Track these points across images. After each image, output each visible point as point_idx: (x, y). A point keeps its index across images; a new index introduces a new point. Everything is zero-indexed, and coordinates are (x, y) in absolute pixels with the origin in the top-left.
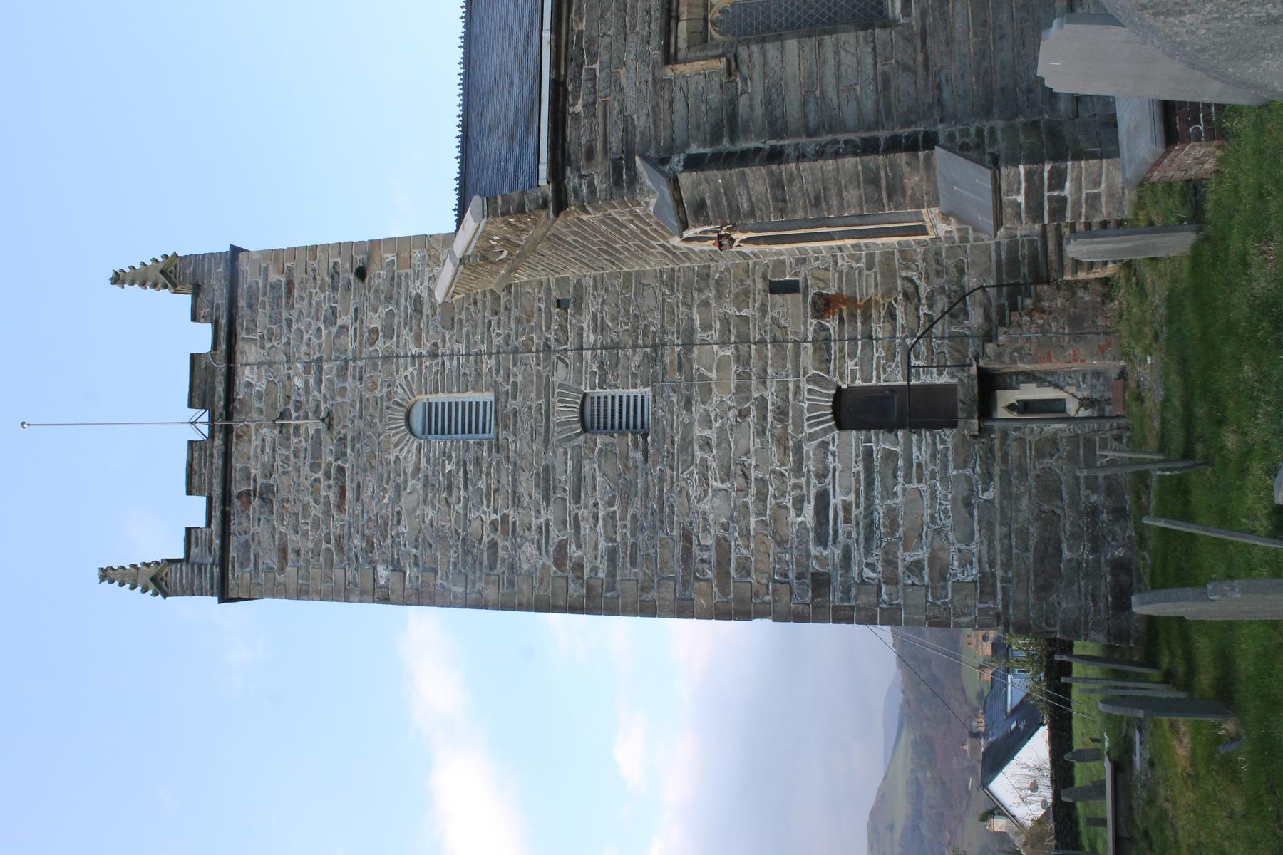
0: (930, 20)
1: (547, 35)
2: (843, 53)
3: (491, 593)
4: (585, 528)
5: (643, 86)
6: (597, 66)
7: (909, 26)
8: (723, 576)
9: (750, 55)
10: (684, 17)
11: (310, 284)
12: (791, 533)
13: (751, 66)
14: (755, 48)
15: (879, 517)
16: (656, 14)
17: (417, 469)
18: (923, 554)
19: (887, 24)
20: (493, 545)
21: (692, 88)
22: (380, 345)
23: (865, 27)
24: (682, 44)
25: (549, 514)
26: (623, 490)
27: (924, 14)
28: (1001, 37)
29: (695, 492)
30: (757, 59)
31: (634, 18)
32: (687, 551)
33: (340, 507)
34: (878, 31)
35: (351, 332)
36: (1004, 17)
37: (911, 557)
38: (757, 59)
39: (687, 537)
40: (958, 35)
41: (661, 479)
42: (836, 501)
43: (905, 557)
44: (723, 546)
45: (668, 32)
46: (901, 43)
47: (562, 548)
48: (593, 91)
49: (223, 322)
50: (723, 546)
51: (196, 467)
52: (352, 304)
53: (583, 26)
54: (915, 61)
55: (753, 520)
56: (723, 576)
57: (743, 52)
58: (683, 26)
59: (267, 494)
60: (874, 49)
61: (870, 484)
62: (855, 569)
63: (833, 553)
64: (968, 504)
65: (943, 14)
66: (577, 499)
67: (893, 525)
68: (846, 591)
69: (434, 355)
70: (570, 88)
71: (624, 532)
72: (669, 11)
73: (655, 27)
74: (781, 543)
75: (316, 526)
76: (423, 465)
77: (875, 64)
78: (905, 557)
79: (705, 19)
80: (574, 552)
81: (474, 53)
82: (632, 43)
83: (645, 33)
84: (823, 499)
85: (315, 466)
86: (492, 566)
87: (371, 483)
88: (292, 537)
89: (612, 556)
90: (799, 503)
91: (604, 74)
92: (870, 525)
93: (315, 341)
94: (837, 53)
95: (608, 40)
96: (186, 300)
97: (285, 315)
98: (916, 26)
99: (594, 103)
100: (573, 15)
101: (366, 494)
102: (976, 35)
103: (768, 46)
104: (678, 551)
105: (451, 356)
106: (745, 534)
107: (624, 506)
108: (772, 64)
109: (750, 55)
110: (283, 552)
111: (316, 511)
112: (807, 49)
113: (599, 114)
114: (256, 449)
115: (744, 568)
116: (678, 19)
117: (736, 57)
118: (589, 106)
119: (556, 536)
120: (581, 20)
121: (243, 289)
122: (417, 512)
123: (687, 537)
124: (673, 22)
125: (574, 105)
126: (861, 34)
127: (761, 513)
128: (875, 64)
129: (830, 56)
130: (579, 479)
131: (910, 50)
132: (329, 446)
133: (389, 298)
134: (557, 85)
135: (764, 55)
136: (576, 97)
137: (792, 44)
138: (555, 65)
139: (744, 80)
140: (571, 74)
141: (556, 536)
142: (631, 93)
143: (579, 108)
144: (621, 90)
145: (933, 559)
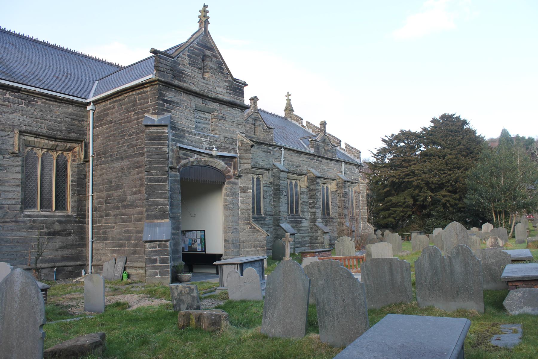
0: (21, 224)
1: (39, 90)
2: (14, 193)
5: (12, 121)
6: (23, 106)
7: (20, 217)
9: (18, 161)
10: (36, 140)
13: (14, 161)
14: (20, 163)
16: (39, 130)
19: (22, 209)
21: (9, 139)
23: (22, 202)
24: (26, 138)
27: (24, 222)
28: (12, 248)
30: (16, 164)
31: (39, 122)
34: (20, 206)
36: (19, 249)
38: (16, 164)
40: (14, 233)
45: (31, 133)
46: (14, 214)
48: (14, 103)
53: (39, 103)
54: (7, 218)
57: (19, 159)
58: (33, 139)
60: (14, 204)
65: (23, 228)
70: (17, 94)
72: (39, 135)
73: (34, 129)
77: (8, 205)
79: (34, 147)
81: (41, 46)
82: (30, 120)
83: (32, 125)
91: (20, 107)
94: (14, 191)
95: (33, 111)
98: (19, 219)
99: (9, 102)
100: (44, 100)
102: (13, 239)
103: (20, 168)
108: (13, 168)
109: (18, 161)
112: (17, 181)
113: (4, 103)
116: (35, 137)
117: (18, 156)
118: (8, 100)
120: (42, 103)
124: (35, 136)
125: (10, 94)
126: (20, 200)
128: (8, 205)
129: (13, 189)
131: (11, 217)
134: (19, 90)
135: (17, 166)
136: (12, 96)
137: (20, 176)
138: (27, 91)
139: (9, 158)
140: (22, 95)
142: (11, 116)
143: (8, 96)
144: (12, 113)
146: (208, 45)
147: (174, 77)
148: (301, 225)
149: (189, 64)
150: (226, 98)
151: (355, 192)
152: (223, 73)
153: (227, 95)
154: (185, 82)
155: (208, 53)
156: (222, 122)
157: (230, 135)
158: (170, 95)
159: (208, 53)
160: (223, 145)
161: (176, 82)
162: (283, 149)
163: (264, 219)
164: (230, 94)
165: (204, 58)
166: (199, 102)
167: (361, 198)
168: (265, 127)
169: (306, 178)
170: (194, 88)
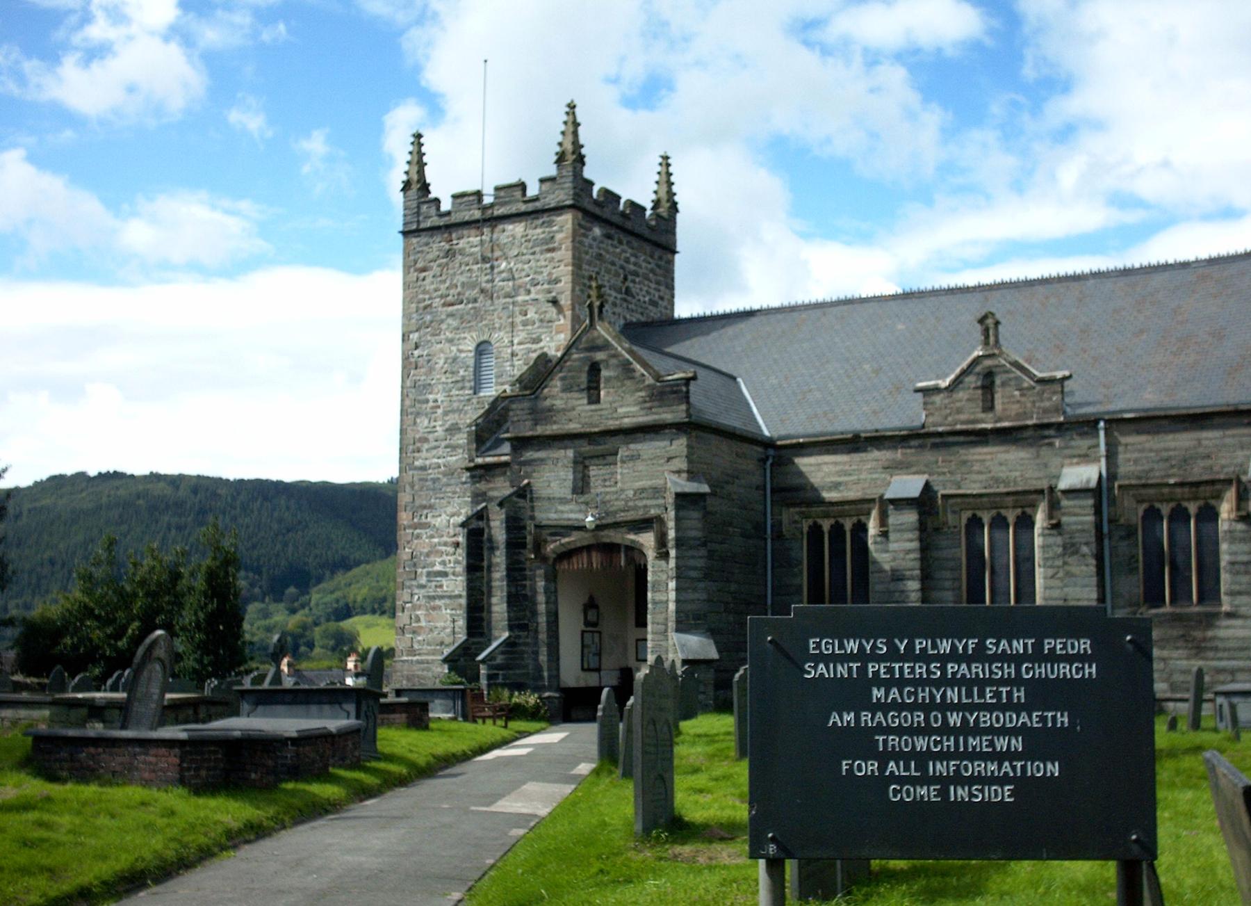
3: (407, 402)
4: (434, 452)
11: (552, 264)
12: (432, 559)
15: (438, 602)
17: (460, 351)
18: (423, 624)
20: (427, 401)
22: (519, 319)
26: (450, 473)
29: (450, 510)
32: (425, 507)
33: (444, 305)
35: (527, 298)
37: (422, 618)
39: (431, 507)
41: (454, 493)
42: (444, 582)
47: (426, 440)
49: (538, 205)
51: (466, 199)
52: (539, 297)
55: (436, 540)
59: (450, 254)
61: (450, 597)
62: (416, 591)
63: (423, 580)
64: (442, 643)
66: (446, 447)
67: (434, 608)
68: (409, 587)
69: (513, 355)
71: (433, 474)
74: (428, 555)
75: (436, 290)
76: (463, 355)
80: (426, 446)
84: (445, 574)
85: (463, 284)
86: (419, 402)
87: (454, 323)
88: (431, 273)
89: (423, 468)
90: (443, 563)
92: (434, 598)
93: (524, 274)
96: (552, 171)
97: (537, 249)
101: (450, 321)
104: (424, 502)
105: (513, 366)
106: (432, 537)
107: (445, 474)
111: (443, 291)
114: (470, 242)
115: (418, 537)
119: (431, 437)
122: (441, 353)
123: (431, 507)
127: (440, 544)
133: (541, 321)
141: (431, 437)
145: (421, 627)
146: (599, 342)
148: (1210, 634)
149: (564, 390)
152: (633, 378)
153: (642, 413)
154: (555, 422)
155: (600, 356)
156: (631, 464)
159: (600, 356)
160: (631, 504)
161: (540, 430)
162: (1102, 424)
164: (650, 408)
165: (594, 369)
168: (1028, 382)
170: (574, 427)
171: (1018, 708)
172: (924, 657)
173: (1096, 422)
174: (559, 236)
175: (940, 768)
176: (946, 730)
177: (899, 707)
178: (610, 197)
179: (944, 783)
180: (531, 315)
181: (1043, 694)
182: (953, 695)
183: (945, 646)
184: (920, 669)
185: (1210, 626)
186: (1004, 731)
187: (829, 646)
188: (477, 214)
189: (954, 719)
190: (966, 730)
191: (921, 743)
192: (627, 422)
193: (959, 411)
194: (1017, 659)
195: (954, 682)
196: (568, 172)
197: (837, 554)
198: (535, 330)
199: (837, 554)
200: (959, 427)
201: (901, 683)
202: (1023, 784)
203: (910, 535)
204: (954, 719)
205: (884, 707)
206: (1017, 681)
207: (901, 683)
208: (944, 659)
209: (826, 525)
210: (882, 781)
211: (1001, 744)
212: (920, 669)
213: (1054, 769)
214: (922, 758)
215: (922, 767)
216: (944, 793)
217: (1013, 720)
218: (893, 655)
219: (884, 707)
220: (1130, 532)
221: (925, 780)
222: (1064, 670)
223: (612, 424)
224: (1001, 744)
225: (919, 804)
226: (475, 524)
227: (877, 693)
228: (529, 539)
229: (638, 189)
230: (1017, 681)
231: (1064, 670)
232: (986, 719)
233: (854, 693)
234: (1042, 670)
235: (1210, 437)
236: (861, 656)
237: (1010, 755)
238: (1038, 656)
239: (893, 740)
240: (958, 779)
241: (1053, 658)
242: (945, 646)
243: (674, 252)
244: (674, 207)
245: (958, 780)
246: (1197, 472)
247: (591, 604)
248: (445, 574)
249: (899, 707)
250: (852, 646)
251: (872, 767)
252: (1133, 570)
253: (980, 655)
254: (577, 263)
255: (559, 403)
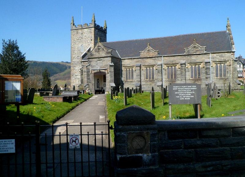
8: (73, 69)
25: (76, 57)
26: (78, 62)
43: (74, 81)
44: (75, 69)
50: (75, 69)
56: (73, 69)
59: (77, 33)
63: (74, 76)
71: (75, 62)
78: (74, 81)
84: (77, 75)
110: (73, 35)
121: (91, 28)
123: (75, 67)
130: (78, 59)
132: (80, 38)
147: (91, 56)
150: (105, 56)
151: (227, 66)
155: (100, 48)
157: (106, 64)
158: (90, 60)
159: (100, 48)
163: (154, 81)
165: (99, 49)
166: (98, 59)
167: (232, 68)
168: (153, 52)
169: (178, 65)
170: (96, 57)
171: (190, 92)
172: (183, 88)
173: (161, 57)
174: (92, 31)
175: (184, 97)
176: (185, 94)
177: (181, 92)
178: (98, 26)
179: (184, 98)
180: (89, 41)
181: (192, 90)
182: (185, 91)
183: (184, 87)
184: (182, 89)
185: (175, 81)
186: (189, 94)
187: (175, 87)
188: (81, 28)
189: (185, 93)
190: (186, 94)
191: (183, 95)
192: (103, 56)
193: (145, 55)
194: (190, 88)
195: (185, 90)
196: (93, 23)
197: (129, 73)
198: (89, 44)
199: (129, 73)
200: (145, 57)
201: (181, 90)
202: (191, 98)
203: (139, 71)
204: (185, 93)
205: (180, 92)
206: (190, 89)
207: (181, 90)
208: (184, 88)
209: (128, 69)
210: (180, 98)
211: (189, 95)
212: (182, 89)
213: (193, 96)
214: (183, 96)
215: (183, 97)
216: (184, 99)
217: (191, 93)
218: (180, 87)
219: (180, 92)
220: (166, 70)
221: (183, 98)
222: (194, 88)
223: (101, 56)
224: (189, 95)
225: (183, 100)
226: (82, 69)
227: (179, 91)
228: (90, 71)
229: (102, 25)
230: (190, 89)
231: (194, 88)
232: (188, 93)
233: (177, 91)
234: (192, 88)
235: (176, 58)
236: (178, 88)
237: (190, 95)
238: (192, 87)
239: (180, 95)
240: (185, 98)
241: (193, 87)
242: (184, 87)
243: (106, 33)
244: (106, 28)
245: (185, 98)
246: (174, 63)
247: (98, 80)
248: (77, 75)
249: (181, 92)
250: (177, 87)
251: (179, 97)
252: (166, 75)
253: (187, 87)
254: (95, 35)
255: (94, 54)
